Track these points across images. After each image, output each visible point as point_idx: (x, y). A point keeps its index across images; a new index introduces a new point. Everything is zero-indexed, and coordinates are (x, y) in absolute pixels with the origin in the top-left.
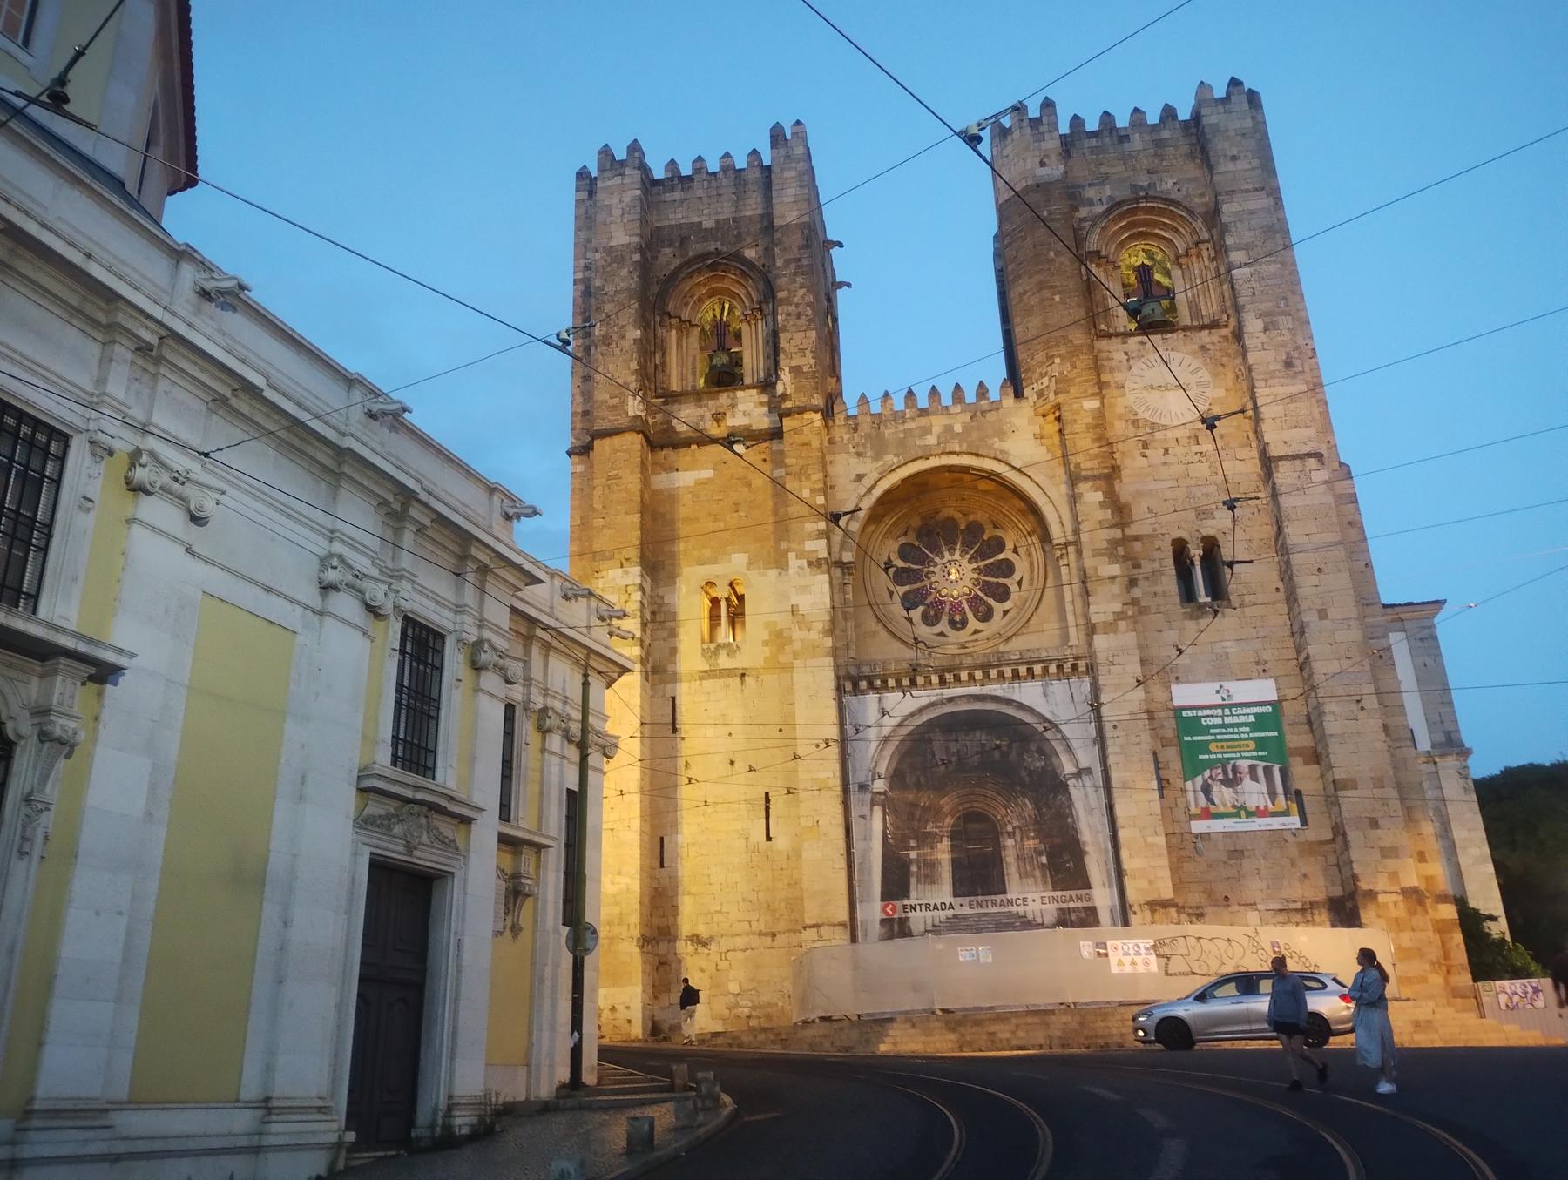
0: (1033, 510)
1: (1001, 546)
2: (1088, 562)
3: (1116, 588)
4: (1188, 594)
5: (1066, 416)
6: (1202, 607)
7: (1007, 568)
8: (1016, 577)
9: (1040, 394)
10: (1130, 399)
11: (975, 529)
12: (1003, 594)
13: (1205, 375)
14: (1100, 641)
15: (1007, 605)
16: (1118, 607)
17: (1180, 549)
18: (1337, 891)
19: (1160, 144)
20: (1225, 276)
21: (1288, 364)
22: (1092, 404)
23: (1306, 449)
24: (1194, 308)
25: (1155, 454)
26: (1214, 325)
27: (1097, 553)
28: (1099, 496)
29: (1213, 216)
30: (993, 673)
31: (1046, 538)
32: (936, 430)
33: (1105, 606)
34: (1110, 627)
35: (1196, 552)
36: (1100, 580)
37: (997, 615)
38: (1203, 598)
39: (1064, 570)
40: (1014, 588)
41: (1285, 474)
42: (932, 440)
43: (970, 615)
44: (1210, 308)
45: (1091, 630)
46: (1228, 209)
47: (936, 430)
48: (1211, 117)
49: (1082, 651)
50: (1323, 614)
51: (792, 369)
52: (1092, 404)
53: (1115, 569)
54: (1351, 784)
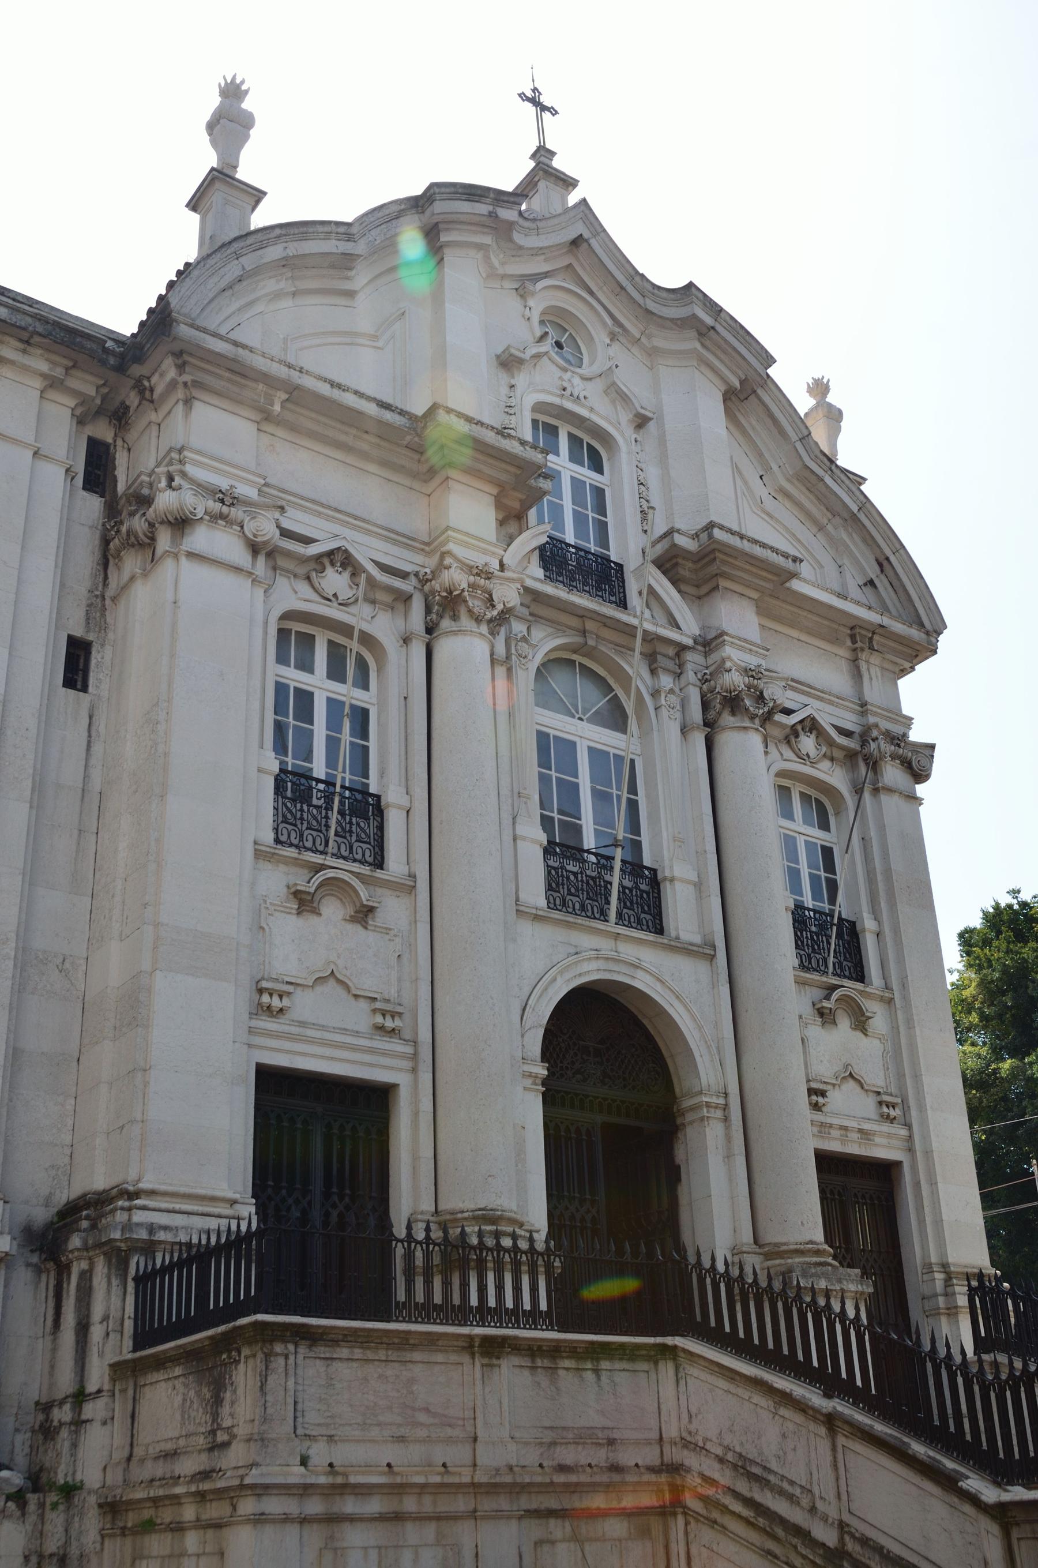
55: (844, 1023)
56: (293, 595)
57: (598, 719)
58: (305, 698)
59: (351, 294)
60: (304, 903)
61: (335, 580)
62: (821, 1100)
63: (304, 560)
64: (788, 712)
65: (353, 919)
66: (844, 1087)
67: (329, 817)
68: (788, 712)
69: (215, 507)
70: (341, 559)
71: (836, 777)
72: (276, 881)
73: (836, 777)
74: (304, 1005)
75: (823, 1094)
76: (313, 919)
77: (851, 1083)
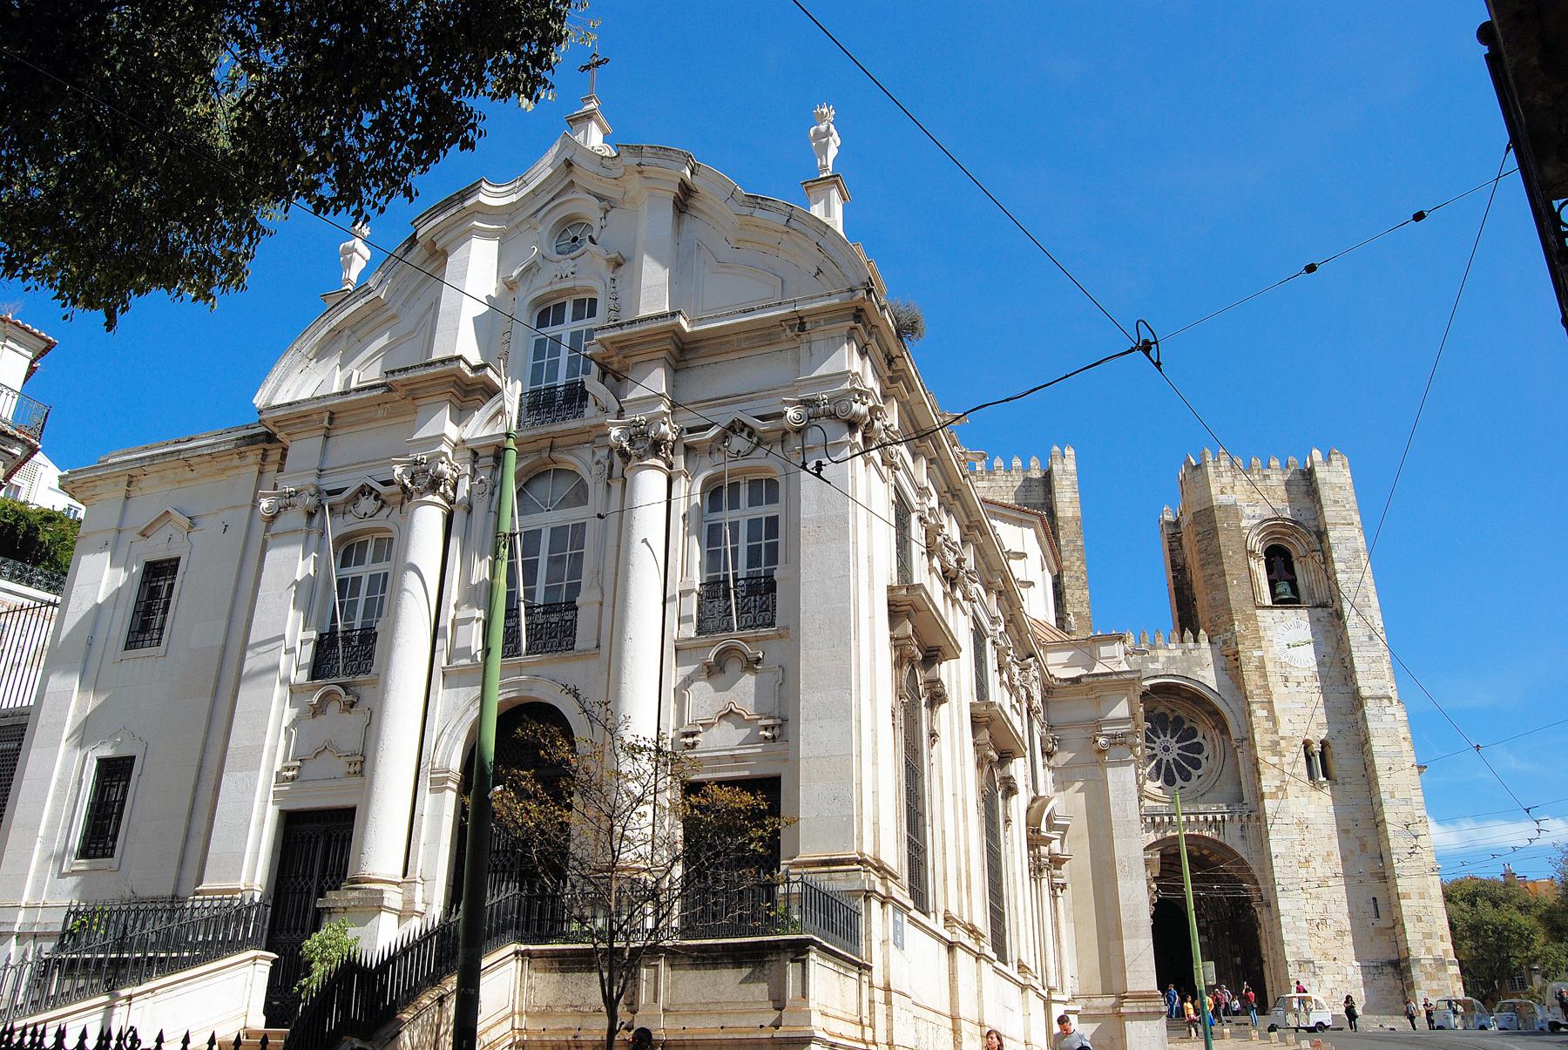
0: (1215, 713)
4: (1311, 776)
6: (1320, 783)
7: (1199, 748)
8: (1205, 754)
9: (1225, 642)
11: (1179, 721)
15: (1200, 772)
16: (1278, 783)
17: (1307, 744)
18: (1394, 957)
21: (1371, 638)
23: (1380, 693)
24: (1311, 595)
26: (1323, 606)
27: (1264, 748)
28: (1265, 713)
29: (1321, 535)
30: (1201, 818)
31: (1224, 729)
32: (1162, 659)
34: (1274, 796)
35: (1317, 748)
37: (1194, 778)
38: (1322, 779)
40: (1204, 761)
42: (1158, 666)
46: (1333, 535)
47: (1162, 659)
49: (1254, 806)
50: (1392, 797)
52: (1257, 653)
57: (565, 503)
59: (394, 317)
61: (367, 504)
62: (690, 740)
63: (347, 502)
69: (282, 502)
70: (365, 491)
71: (767, 462)
73: (767, 462)
75: (693, 734)
76: (320, 718)
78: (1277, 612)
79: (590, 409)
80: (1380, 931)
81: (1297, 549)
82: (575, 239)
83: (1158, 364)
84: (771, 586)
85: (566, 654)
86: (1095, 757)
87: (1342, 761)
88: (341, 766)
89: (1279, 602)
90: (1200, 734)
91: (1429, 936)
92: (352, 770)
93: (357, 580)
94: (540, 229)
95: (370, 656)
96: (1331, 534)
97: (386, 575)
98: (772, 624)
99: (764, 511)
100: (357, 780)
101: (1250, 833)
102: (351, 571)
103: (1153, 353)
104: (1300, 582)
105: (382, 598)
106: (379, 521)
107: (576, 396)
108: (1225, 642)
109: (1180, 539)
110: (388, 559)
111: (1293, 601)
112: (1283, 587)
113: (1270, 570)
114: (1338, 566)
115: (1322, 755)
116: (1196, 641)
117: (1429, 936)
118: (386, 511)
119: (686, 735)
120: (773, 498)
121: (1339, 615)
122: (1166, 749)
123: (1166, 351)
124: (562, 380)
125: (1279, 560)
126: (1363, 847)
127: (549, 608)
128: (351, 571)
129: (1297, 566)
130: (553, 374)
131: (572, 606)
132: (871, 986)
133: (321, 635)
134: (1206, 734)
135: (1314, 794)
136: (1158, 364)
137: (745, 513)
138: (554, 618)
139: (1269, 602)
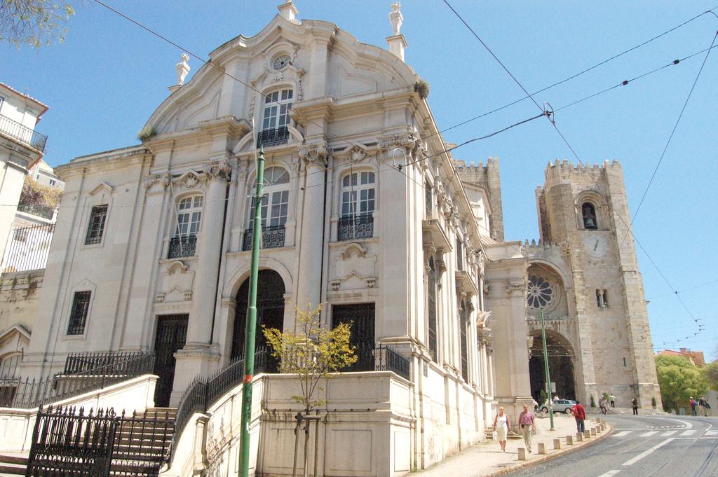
1: (547, 285)
2: (577, 294)
3: (583, 303)
4: (599, 305)
5: (571, 252)
7: (549, 292)
10: (586, 248)
11: (541, 280)
12: (549, 299)
13: (605, 244)
14: (579, 316)
15: (550, 302)
17: (597, 291)
18: (632, 383)
19: (593, 174)
20: (611, 217)
22: (577, 250)
25: (592, 266)
26: (607, 230)
27: (578, 292)
29: (608, 198)
30: (550, 322)
31: (561, 282)
33: (580, 307)
34: (582, 313)
36: (579, 300)
37: (547, 305)
39: (568, 295)
41: (627, 276)
43: (540, 304)
44: (607, 225)
45: (577, 313)
46: (613, 199)
48: (608, 171)
50: (634, 314)
51: (497, 232)
52: (577, 250)
53: (584, 297)
54: (638, 357)
55: (354, 257)
56: (179, 192)
57: (280, 182)
58: (187, 215)
60: (172, 271)
62: (335, 287)
63: (182, 180)
64: (343, 149)
65: (183, 272)
66: (351, 279)
67: (180, 246)
68: (343, 149)
70: (190, 176)
71: (370, 164)
72: (164, 269)
74: (168, 298)
76: (173, 275)
77: (354, 277)
78: (587, 232)
79: (290, 140)
80: (626, 372)
81: (597, 204)
82: (282, 63)
83: (553, 122)
84: (371, 219)
85: (281, 248)
86: (506, 295)
87: (613, 298)
88: (182, 297)
89: (588, 227)
90: (550, 285)
91: (647, 375)
92: (187, 297)
93: (187, 215)
94: (267, 58)
95: (194, 248)
96: (612, 198)
97: (200, 213)
98: (371, 237)
99: (368, 186)
100: (190, 302)
101: (571, 328)
102: (184, 211)
103: (551, 116)
104: (598, 219)
105: (199, 223)
106: (197, 189)
107: (284, 133)
108: (563, 245)
109: (545, 199)
110: (201, 206)
111: (594, 228)
112: (590, 222)
113: (584, 214)
114: (615, 213)
115: (604, 296)
116: (550, 244)
117: (647, 375)
118: (199, 185)
119: (333, 284)
120: (372, 181)
121: (614, 234)
122: (535, 292)
123: (556, 116)
124: (277, 126)
125: (588, 209)
126: (620, 336)
127: (273, 228)
128: (184, 211)
129: (596, 212)
130: (273, 124)
131: (283, 227)
132: (414, 393)
133: (172, 239)
134: (553, 286)
135: (600, 313)
136: (553, 122)
137: (359, 187)
138: (275, 232)
139: (583, 227)
